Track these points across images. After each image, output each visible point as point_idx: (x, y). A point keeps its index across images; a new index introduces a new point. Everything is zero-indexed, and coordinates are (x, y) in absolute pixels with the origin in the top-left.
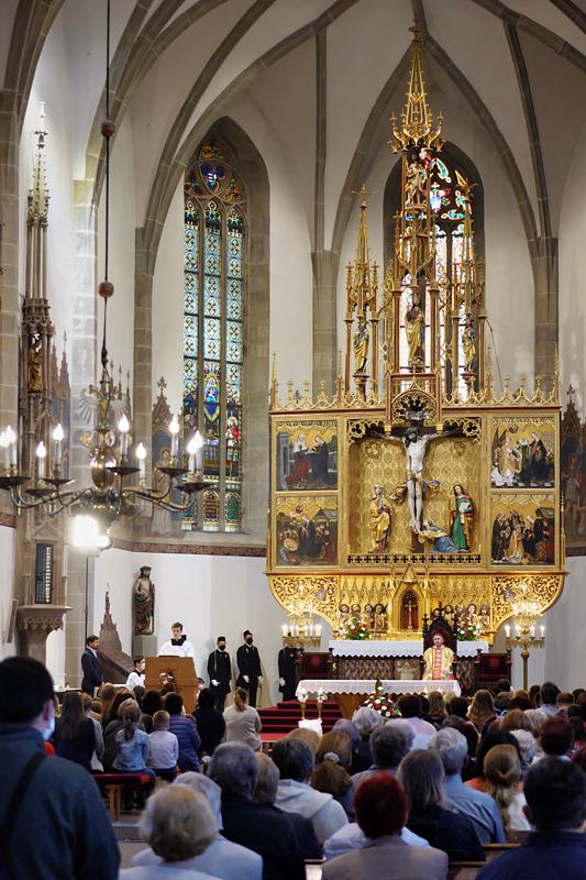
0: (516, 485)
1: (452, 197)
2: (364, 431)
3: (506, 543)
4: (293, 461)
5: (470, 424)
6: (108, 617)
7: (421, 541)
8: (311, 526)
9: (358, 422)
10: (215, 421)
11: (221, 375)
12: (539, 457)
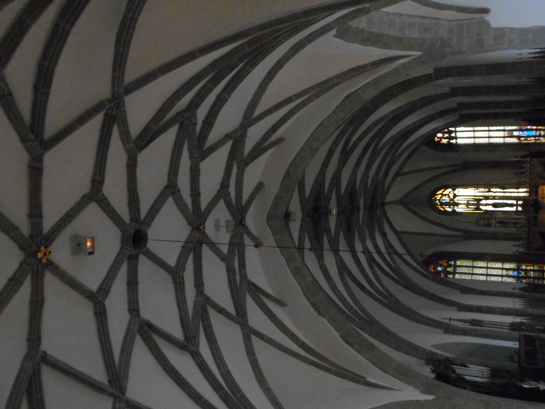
1: (445, 195)
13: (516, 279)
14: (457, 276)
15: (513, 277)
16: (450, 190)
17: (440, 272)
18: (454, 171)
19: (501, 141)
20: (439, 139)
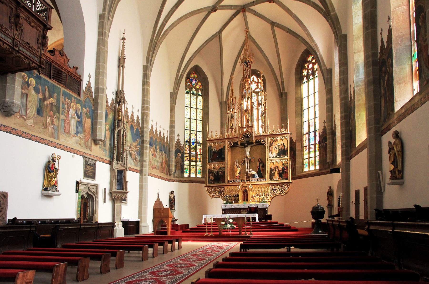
0: (276, 157)
1: (258, 85)
2: (232, 144)
3: (274, 174)
4: (213, 154)
5: (263, 140)
7: (249, 176)
8: (218, 172)
9: (231, 142)
10: (194, 147)
11: (196, 135)
12: (283, 148)
13: (188, 140)
17: (191, 83)
18: (278, 85)
20: (307, 67)
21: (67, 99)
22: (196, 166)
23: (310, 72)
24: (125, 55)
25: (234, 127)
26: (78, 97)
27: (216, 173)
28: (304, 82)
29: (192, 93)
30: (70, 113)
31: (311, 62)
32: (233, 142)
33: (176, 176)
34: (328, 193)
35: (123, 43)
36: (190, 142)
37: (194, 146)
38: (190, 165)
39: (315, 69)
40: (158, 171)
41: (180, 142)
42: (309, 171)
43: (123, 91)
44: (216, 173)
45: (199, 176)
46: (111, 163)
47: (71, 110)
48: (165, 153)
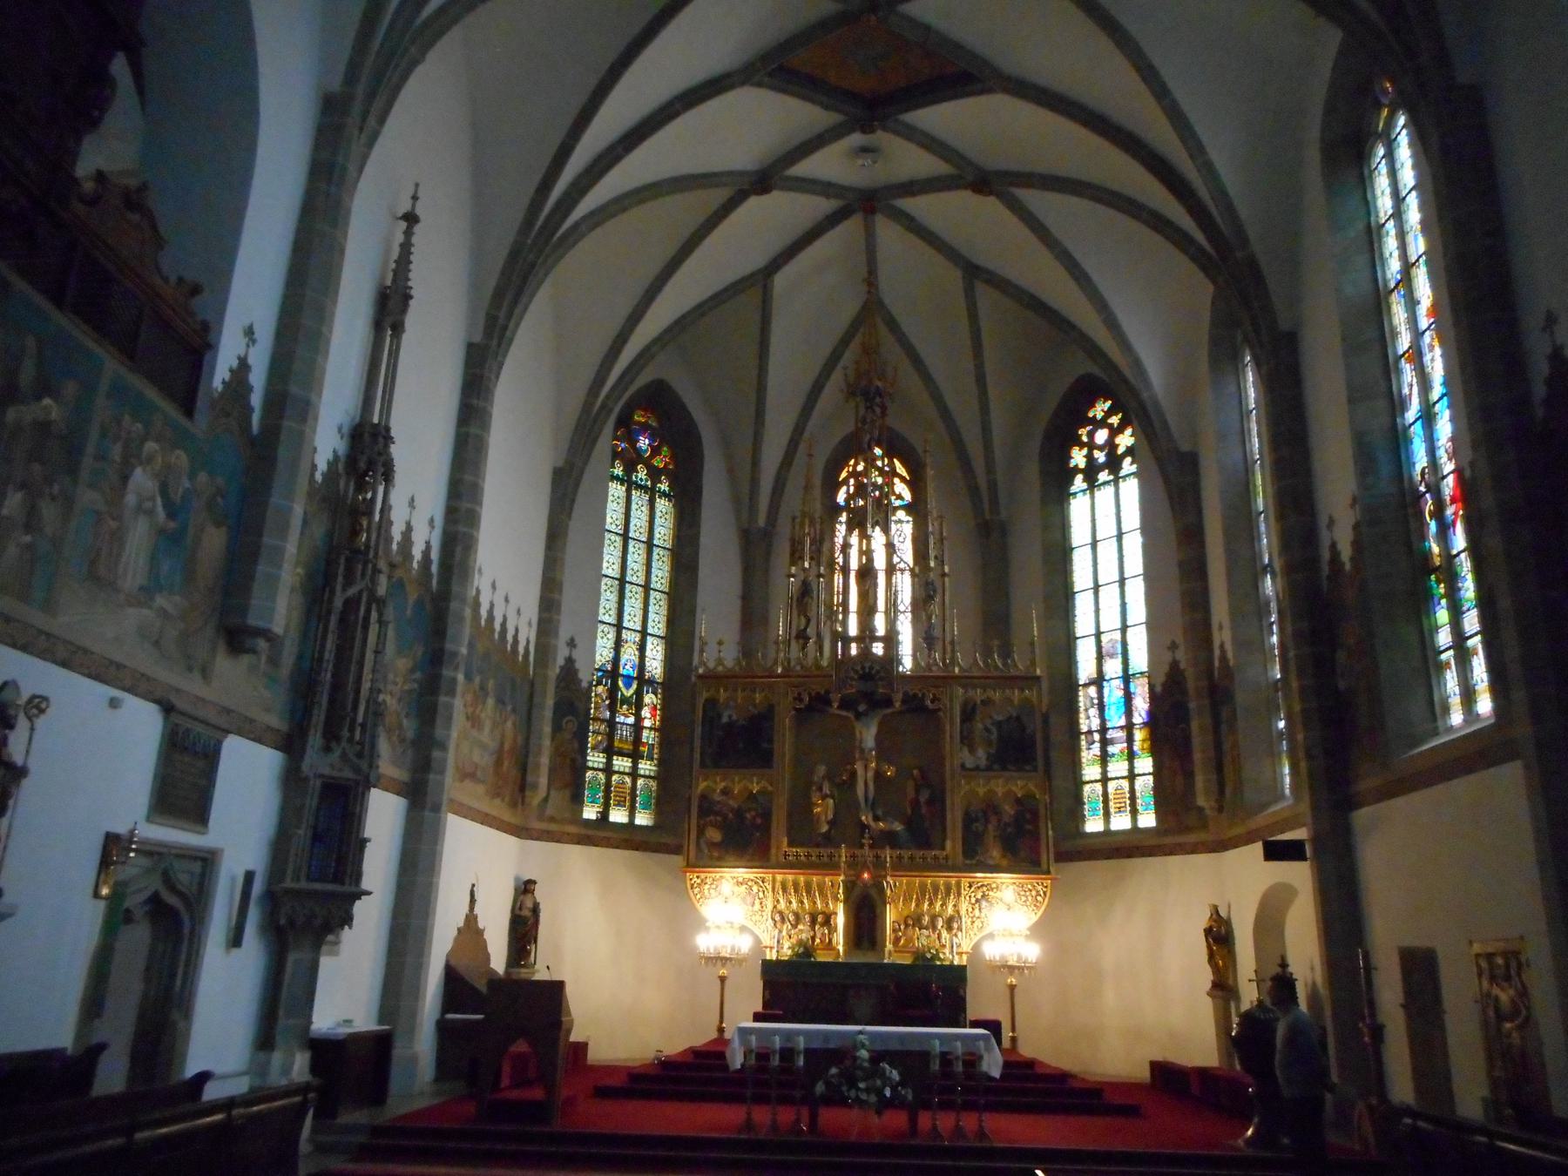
0: (989, 768)
5: (934, 695)
6: (471, 919)
8: (739, 813)
11: (642, 648)
14: (616, 491)
15: (616, 661)
16: (907, 496)
18: (974, 491)
19: (1083, 623)
20: (1085, 439)
21: (127, 417)
22: (634, 774)
23: (1100, 457)
24: (410, 284)
25: (811, 631)
26: (182, 420)
27: (731, 815)
28: (1073, 489)
29: (636, 483)
30: (131, 485)
31: (1102, 423)
32: (810, 694)
33: (550, 811)
34: (1208, 932)
35: (408, 233)
36: (613, 673)
37: (629, 693)
38: (608, 770)
39: (1121, 450)
40: (481, 789)
41: (576, 672)
42: (1107, 832)
43: (388, 429)
44: (731, 815)
45: (643, 819)
46: (291, 744)
47: (138, 471)
48: (514, 710)
